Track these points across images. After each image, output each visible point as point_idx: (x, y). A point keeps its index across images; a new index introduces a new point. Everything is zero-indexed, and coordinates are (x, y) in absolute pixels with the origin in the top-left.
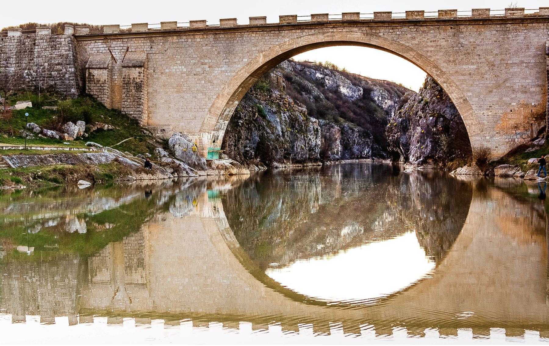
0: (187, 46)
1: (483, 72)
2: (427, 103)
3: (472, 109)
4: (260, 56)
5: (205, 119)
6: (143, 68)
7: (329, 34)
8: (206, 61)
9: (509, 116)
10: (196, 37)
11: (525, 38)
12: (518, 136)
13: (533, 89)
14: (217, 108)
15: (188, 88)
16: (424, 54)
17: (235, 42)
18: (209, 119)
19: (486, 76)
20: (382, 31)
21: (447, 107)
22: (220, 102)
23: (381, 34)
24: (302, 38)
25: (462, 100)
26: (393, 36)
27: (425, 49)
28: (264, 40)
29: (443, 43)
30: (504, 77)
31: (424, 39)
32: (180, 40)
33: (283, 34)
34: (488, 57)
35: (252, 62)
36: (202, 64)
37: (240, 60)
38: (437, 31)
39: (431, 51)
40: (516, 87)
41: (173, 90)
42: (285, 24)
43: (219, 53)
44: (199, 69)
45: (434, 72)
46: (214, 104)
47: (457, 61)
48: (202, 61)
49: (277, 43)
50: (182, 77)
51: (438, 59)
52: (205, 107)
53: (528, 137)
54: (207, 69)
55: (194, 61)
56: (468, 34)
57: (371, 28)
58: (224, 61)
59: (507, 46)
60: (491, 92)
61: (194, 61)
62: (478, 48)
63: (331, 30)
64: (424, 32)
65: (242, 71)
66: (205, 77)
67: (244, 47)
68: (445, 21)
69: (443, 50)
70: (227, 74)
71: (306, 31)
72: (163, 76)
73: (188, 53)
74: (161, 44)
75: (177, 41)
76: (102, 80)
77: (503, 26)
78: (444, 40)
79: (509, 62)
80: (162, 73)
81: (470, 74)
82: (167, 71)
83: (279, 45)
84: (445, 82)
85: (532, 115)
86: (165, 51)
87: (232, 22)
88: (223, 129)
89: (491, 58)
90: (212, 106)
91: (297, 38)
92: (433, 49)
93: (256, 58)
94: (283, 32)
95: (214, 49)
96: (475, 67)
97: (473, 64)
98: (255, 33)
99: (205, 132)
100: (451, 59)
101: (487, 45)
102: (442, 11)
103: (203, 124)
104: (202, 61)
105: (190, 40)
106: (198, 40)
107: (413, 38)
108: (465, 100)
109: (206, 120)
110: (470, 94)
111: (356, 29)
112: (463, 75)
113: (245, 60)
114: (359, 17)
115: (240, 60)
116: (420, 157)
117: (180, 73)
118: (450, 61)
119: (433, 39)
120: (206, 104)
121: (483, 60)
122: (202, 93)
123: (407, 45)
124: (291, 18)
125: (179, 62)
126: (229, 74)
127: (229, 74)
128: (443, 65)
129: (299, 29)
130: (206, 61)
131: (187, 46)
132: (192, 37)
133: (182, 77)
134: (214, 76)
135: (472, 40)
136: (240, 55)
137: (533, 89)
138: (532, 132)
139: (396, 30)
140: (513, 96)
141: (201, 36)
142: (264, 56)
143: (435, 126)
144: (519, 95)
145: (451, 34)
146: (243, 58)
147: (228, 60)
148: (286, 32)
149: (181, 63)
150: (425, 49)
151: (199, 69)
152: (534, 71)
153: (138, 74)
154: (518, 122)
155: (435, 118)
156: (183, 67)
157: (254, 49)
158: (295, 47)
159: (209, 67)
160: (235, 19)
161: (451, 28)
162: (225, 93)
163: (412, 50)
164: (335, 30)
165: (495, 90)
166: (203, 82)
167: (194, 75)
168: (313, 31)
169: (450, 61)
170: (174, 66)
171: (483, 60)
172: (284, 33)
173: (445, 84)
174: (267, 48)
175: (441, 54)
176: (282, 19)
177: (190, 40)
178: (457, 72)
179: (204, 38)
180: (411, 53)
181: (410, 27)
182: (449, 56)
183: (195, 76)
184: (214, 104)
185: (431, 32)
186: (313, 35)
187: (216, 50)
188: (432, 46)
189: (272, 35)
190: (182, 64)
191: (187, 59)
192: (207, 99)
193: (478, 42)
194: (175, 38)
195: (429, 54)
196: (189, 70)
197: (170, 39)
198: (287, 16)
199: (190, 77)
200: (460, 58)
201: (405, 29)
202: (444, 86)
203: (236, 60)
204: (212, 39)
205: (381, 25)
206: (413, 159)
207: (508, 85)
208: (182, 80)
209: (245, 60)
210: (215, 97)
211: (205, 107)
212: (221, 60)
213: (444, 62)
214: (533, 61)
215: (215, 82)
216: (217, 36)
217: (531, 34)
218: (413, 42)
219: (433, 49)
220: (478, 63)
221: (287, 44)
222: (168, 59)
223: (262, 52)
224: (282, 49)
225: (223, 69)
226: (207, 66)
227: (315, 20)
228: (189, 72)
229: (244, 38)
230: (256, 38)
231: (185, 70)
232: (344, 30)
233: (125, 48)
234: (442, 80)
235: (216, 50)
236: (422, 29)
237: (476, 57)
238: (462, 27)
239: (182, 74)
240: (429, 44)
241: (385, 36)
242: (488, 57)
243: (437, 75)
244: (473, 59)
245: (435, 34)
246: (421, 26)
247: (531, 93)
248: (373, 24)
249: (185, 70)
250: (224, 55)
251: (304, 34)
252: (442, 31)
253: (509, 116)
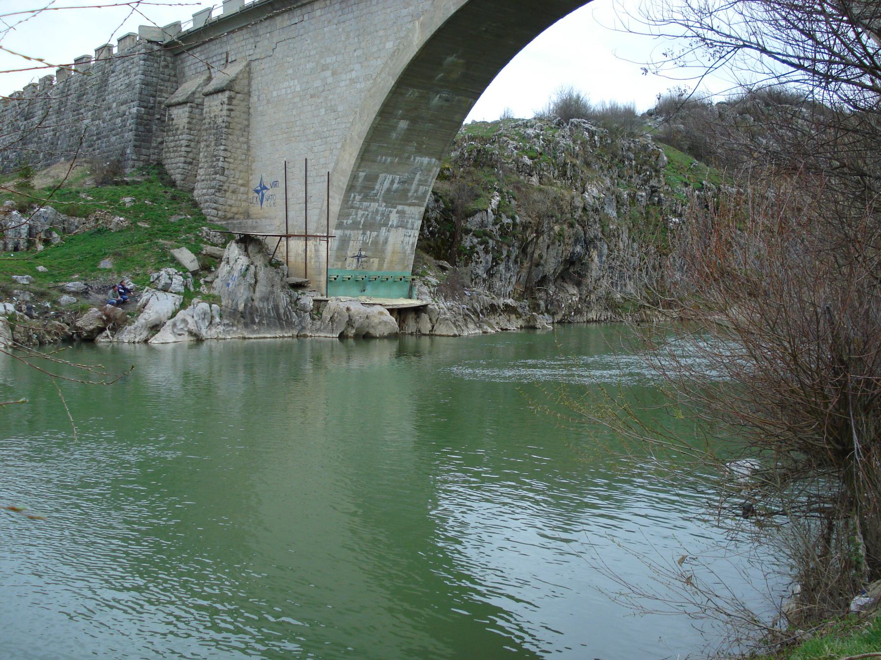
6: (227, 93)
8: (329, 60)
48: (323, 61)
54: (330, 80)
65: (383, 75)
75: (288, 23)
76: (181, 127)
80: (268, 102)
88: (402, 225)
122: (321, 138)
125: (290, 71)
131: (302, 31)
136: (381, 33)
153: (220, 107)
157: (404, 12)
166: (323, 111)
167: (312, 97)
209: (389, 45)
210: (339, 146)
226: (328, 73)
233: (224, 56)
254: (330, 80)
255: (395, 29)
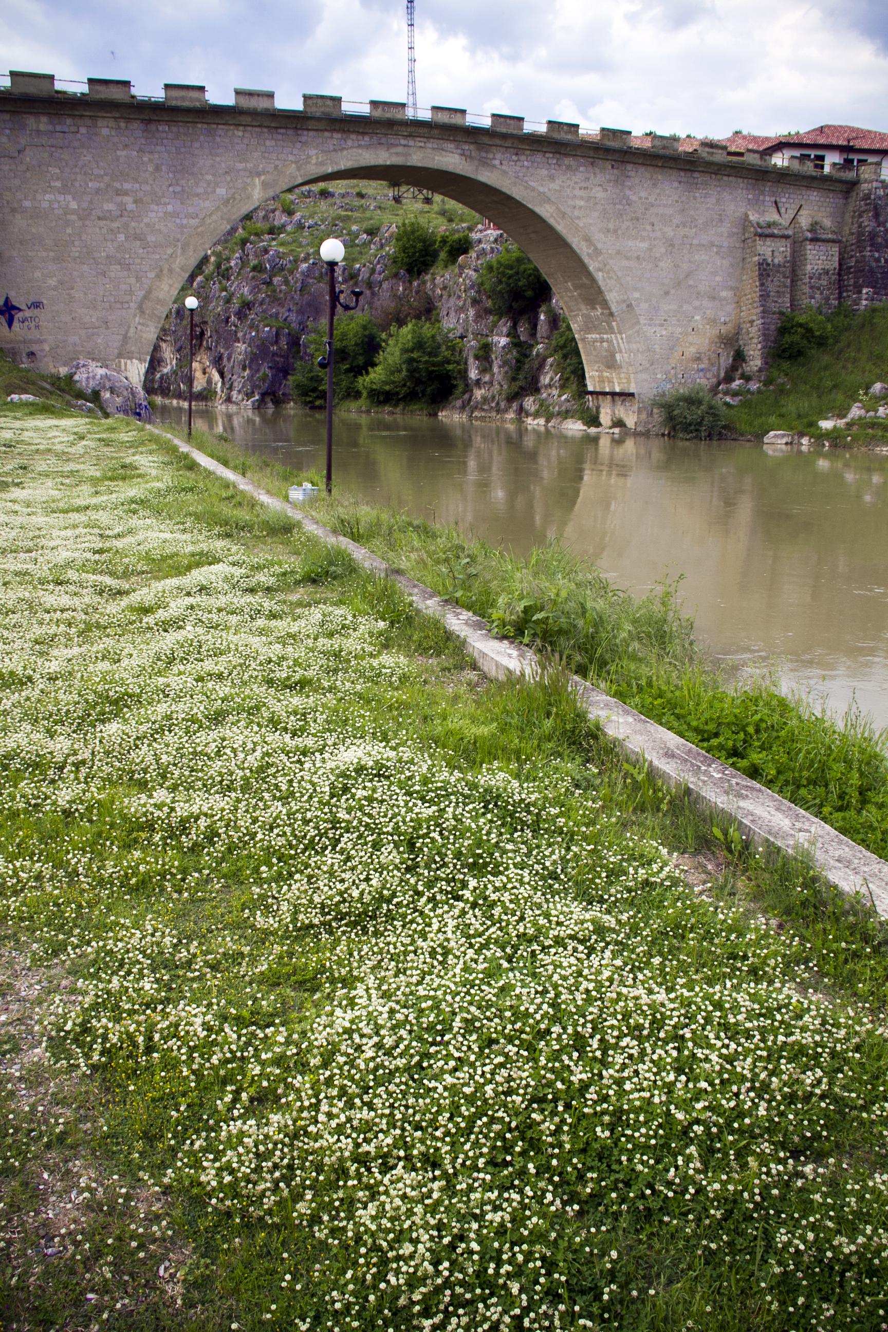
0: (77, 144)
1: (658, 255)
2: (247, 305)
3: (638, 322)
4: (254, 184)
5: (129, 327)
7: (400, 149)
8: (127, 186)
9: (690, 339)
10: (100, 123)
11: (718, 200)
12: (701, 374)
13: (724, 294)
14: (159, 301)
15: (85, 250)
16: (568, 211)
17: (197, 145)
18: (139, 327)
19: (661, 264)
20: (498, 156)
21: (289, 310)
22: (165, 287)
23: (497, 162)
24: (345, 152)
25: (624, 306)
26: (518, 168)
27: (570, 202)
28: (263, 149)
29: (599, 194)
30: (685, 266)
31: (569, 182)
32: (58, 128)
33: (304, 139)
34: (666, 229)
35: (237, 196)
36: (118, 193)
37: (209, 190)
38: (590, 169)
39: (580, 207)
40: (701, 288)
41: (44, 254)
42: (318, 115)
43: (157, 168)
44: (110, 206)
45: (584, 248)
46: (149, 292)
47: (620, 232)
48: (117, 185)
49: (291, 158)
50: (67, 223)
51: (590, 224)
52: (127, 298)
53: (714, 376)
54: (131, 206)
55: (97, 185)
56: (637, 181)
57: (480, 146)
58: (171, 189)
59: (692, 213)
60: (667, 293)
61: (97, 185)
62: (653, 210)
63: (403, 142)
64: (569, 167)
65: (214, 217)
66: (126, 226)
67: (218, 159)
68: (608, 150)
69: (599, 207)
70: (178, 221)
71: (353, 136)
72: (18, 216)
73: (80, 163)
74: (7, 131)
75: (50, 127)
77: (689, 174)
78: (600, 188)
79: (695, 242)
80: (14, 210)
81: (638, 258)
82: (27, 204)
83: (296, 162)
84: (600, 270)
85: (720, 336)
86: (19, 152)
87: (195, 94)
89: (669, 232)
90: (145, 297)
91: (335, 150)
92: (582, 203)
93: (244, 189)
94: (305, 133)
95: (145, 159)
96: (644, 245)
97: (643, 239)
98: (241, 128)
99: (131, 358)
100: (611, 226)
101: (665, 206)
102: (608, 130)
103: (125, 338)
104: (117, 185)
105: (83, 130)
106: (105, 131)
107: (552, 178)
108: (629, 306)
109: (132, 330)
110: (637, 295)
111: (451, 146)
112: (628, 259)
113: (221, 191)
114: (464, 118)
115: (209, 190)
116: (253, 392)
117: (61, 211)
118: (608, 231)
119: (583, 185)
120: (131, 292)
121: (658, 234)
123: (541, 189)
124: (329, 103)
125: (58, 184)
126: (185, 221)
127: (185, 221)
128: (598, 237)
129: (338, 131)
130: (127, 186)
131: (77, 144)
132: (89, 122)
133: (67, 223)
134: (148, 225)
135: (643, 194)
136: (209, 177)
137: (724, 294)
138: (719, 369)
139: (523, 158)
140: (697, 303)
141: (112, 123)
142: (265, 185)
143: (277, 342)
144: (706, 303)
145: (612, 178)
146: (217, 185)
147: (178, 189)
148: (311, 133)
149: (64, 186)
150: (570, 202)
151: (110, 206)
152: (726, 263)
154: (702, 350)
155: (274, 329)
156: (69, 198)
157: (241, 166)
158: (330, 171)
159: (135, 202)
160: (202, 89)
161: (613, 167)
162: (176, 266)
163: (548, 200)
164: (411, 143)
165: (673, 291)
166: (121, 237)
167: (99, 218)
168: (367, 138)
169: (608, 231)
170: (45, 192)
171: (658, 234)
172: (307, 136)
173: (600, 274)
174: (270, 168)
175: (596, 214)
176: (309, 102)
177: (83, 130)
178: (618, 252)
179: (119, 128)
180: (547, 206)
181: (547, 155)
182: (609, 220)
183: (102, 223)
184: (149, 292)
185: (582, 169)
186: (367, 147)
187: (150, 160)
188: (582, 198)
189: (280, 137)
190: (65, 189)
191: (79, 177)
192: (132, 280)
193: (652, 199)
194: (44, 119)
195: (576, 213)
196: (85, 205)
197: (31, 121)
198: (322, 97)
199: (87, 223)
200: (624, 227)
201: (539, 157)
202: (599, 276)
203: (200, 190)
204: (139, 133)
205: (498, 142)
206: (240, 397)
207: (691, 282)
208: (69, 231)
209: (221, 191)
210: (151, 275)
211: (127, 298)
212: (164, 187)
213: (600, 231)
214: (726, 244)
215: (151, 238)
216: (152, 127)
217: (726, 195)
218: (552, 186)
219: (582, 203)
220: (650, 239)
221: (314, 161)
222: (28, 174)
223: (259, 174)
224: (302, 172)
225: (170, 208)
226: (128, 200)
227: (378, 113)
228: (84, 210)
229: (218, 139)
230: (246, 141)
231: (74, 205)
232: (429, 145)
234: (597, 265)
235: (150, 160)
236: (568, 161)
237: (649, 227)
238: (629, 167)
239: (66, 214)
240: (578, 193)
241: (504, 167)
242: (666, 229)
243: (588, 254)
244: (644, 229)
245: (587, 175)
246: (567, 155)
247: (721, 300)
248: (486, 140)
249: (74, 205)
250: (171, 175)
251: (350, 143)
252: (598, 171)
253: (690, 339)
254: (131, 206)
255: (229, 179)
